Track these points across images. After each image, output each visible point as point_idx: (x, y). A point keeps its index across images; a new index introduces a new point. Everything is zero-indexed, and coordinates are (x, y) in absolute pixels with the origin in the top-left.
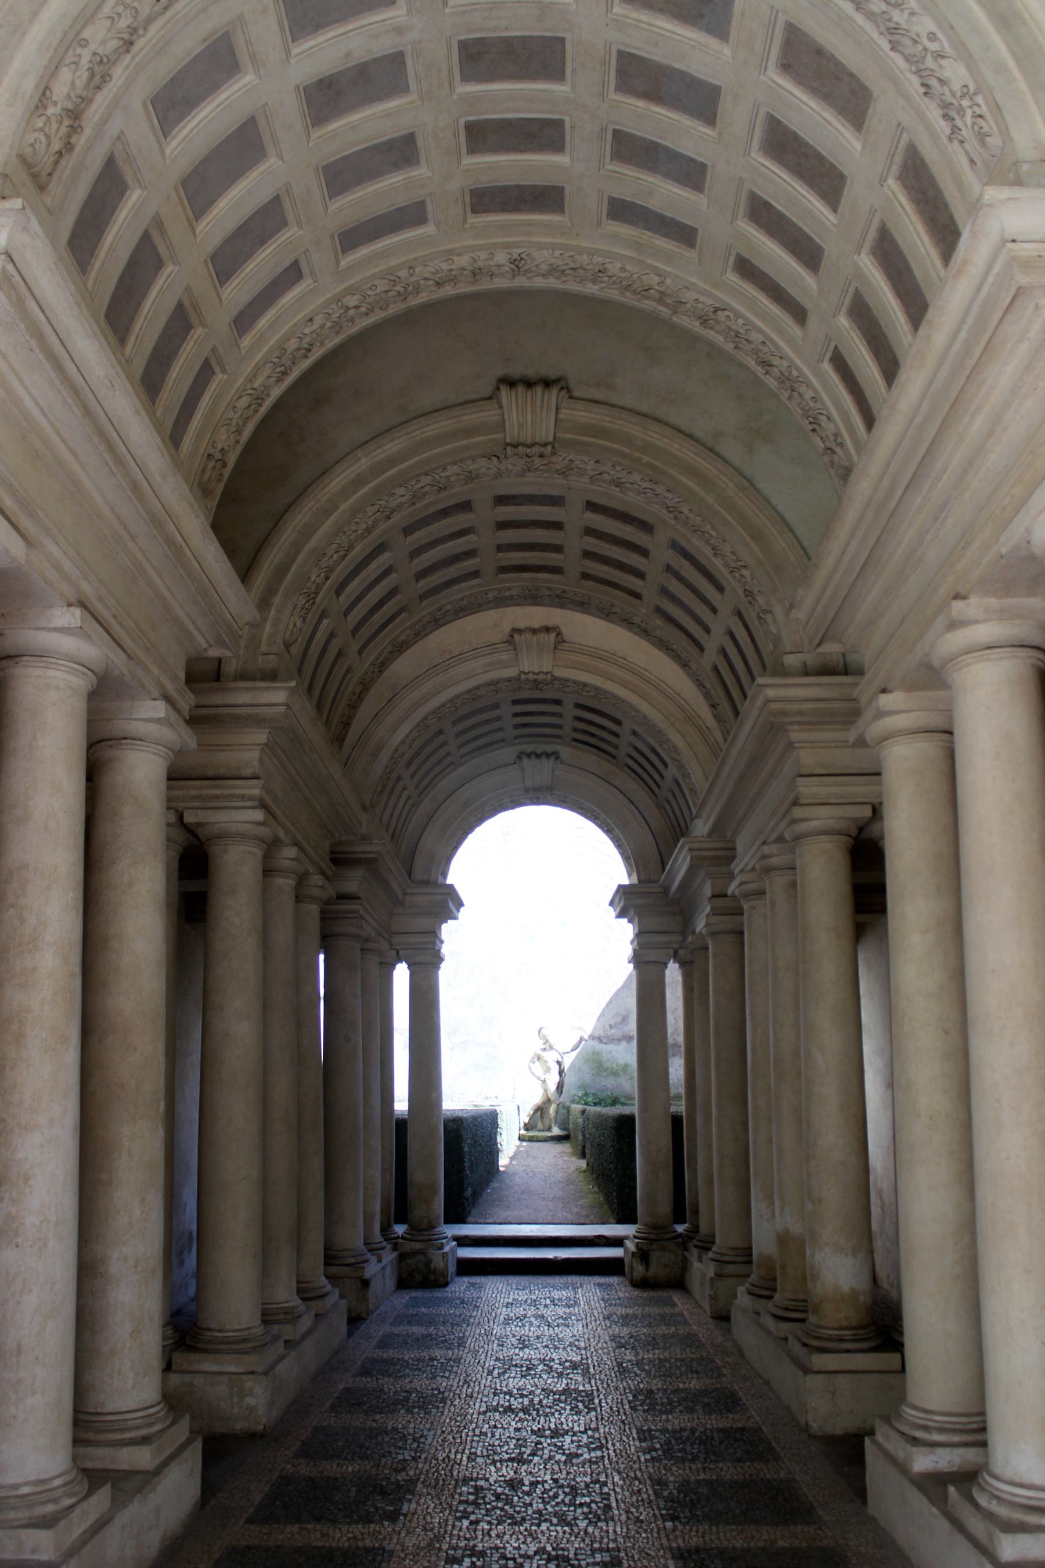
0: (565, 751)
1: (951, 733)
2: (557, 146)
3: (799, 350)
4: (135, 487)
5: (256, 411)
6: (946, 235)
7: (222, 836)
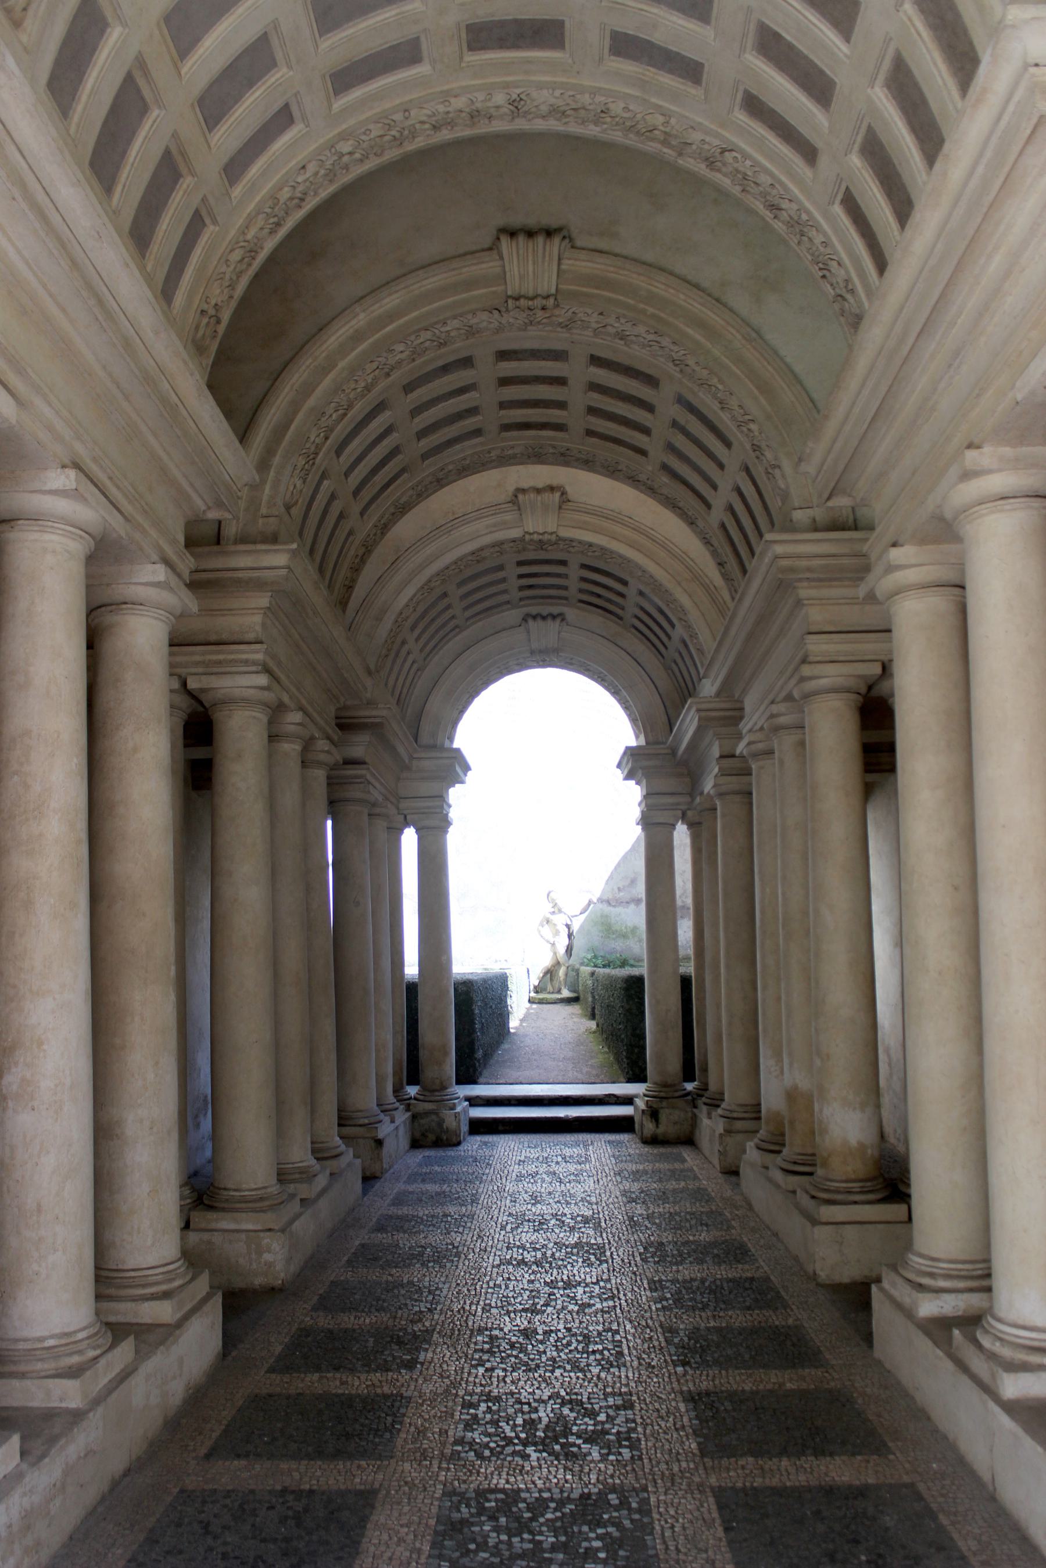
0: (571, 613)
1: (963, 587)
3: (808, 192)
4: (127, 344)
5: (250, 265)
6: (964, 61)
7: (228, 701)
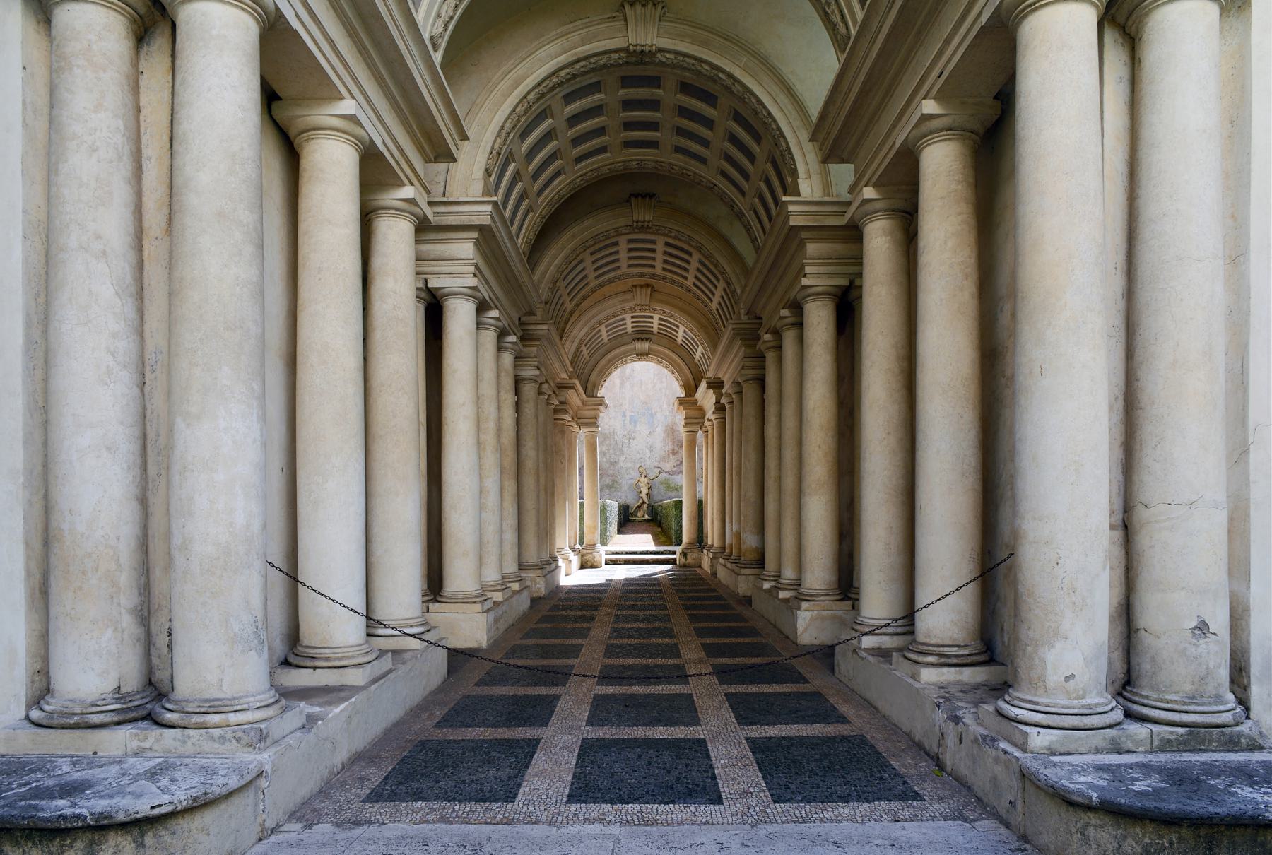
2: (657, 129)
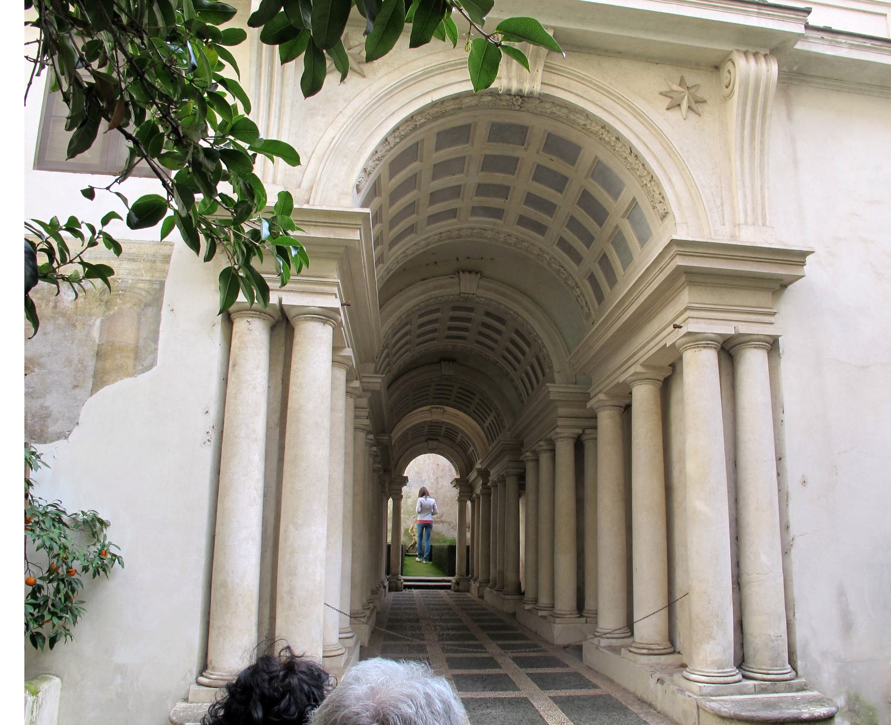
0: (441, 439)
